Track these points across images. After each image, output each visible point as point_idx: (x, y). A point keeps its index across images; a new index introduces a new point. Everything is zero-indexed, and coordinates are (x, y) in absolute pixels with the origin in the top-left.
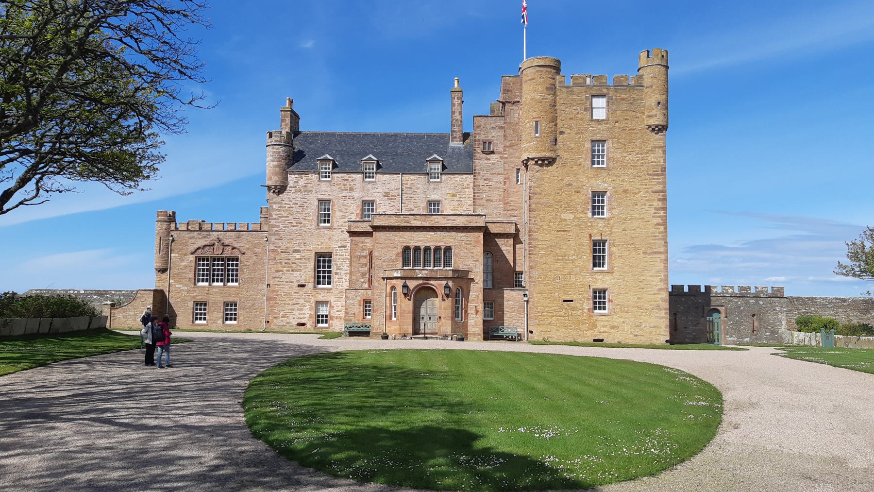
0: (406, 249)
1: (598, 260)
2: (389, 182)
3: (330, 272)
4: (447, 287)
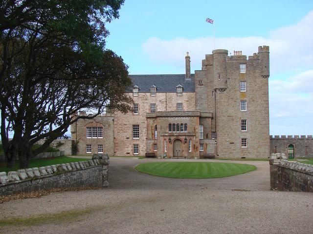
0: (170, 125)
1: (243, 128)
2: (161, 96)
3: (138, 133)
4: (186, 139)
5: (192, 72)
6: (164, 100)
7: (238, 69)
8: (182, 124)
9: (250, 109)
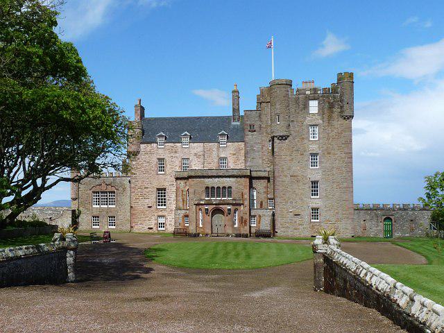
0: (207, 188)
1: (315, 193)
2: (198, 147)
5: (242, 113)
6: (201, 153)
7: (306, 107)
8: (224, 188)
9: (323, 165)
